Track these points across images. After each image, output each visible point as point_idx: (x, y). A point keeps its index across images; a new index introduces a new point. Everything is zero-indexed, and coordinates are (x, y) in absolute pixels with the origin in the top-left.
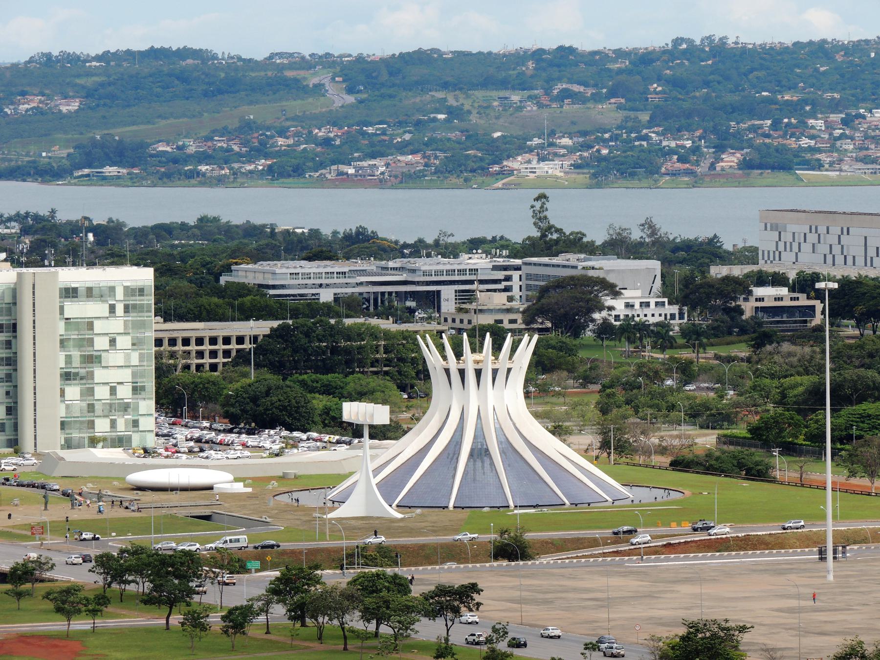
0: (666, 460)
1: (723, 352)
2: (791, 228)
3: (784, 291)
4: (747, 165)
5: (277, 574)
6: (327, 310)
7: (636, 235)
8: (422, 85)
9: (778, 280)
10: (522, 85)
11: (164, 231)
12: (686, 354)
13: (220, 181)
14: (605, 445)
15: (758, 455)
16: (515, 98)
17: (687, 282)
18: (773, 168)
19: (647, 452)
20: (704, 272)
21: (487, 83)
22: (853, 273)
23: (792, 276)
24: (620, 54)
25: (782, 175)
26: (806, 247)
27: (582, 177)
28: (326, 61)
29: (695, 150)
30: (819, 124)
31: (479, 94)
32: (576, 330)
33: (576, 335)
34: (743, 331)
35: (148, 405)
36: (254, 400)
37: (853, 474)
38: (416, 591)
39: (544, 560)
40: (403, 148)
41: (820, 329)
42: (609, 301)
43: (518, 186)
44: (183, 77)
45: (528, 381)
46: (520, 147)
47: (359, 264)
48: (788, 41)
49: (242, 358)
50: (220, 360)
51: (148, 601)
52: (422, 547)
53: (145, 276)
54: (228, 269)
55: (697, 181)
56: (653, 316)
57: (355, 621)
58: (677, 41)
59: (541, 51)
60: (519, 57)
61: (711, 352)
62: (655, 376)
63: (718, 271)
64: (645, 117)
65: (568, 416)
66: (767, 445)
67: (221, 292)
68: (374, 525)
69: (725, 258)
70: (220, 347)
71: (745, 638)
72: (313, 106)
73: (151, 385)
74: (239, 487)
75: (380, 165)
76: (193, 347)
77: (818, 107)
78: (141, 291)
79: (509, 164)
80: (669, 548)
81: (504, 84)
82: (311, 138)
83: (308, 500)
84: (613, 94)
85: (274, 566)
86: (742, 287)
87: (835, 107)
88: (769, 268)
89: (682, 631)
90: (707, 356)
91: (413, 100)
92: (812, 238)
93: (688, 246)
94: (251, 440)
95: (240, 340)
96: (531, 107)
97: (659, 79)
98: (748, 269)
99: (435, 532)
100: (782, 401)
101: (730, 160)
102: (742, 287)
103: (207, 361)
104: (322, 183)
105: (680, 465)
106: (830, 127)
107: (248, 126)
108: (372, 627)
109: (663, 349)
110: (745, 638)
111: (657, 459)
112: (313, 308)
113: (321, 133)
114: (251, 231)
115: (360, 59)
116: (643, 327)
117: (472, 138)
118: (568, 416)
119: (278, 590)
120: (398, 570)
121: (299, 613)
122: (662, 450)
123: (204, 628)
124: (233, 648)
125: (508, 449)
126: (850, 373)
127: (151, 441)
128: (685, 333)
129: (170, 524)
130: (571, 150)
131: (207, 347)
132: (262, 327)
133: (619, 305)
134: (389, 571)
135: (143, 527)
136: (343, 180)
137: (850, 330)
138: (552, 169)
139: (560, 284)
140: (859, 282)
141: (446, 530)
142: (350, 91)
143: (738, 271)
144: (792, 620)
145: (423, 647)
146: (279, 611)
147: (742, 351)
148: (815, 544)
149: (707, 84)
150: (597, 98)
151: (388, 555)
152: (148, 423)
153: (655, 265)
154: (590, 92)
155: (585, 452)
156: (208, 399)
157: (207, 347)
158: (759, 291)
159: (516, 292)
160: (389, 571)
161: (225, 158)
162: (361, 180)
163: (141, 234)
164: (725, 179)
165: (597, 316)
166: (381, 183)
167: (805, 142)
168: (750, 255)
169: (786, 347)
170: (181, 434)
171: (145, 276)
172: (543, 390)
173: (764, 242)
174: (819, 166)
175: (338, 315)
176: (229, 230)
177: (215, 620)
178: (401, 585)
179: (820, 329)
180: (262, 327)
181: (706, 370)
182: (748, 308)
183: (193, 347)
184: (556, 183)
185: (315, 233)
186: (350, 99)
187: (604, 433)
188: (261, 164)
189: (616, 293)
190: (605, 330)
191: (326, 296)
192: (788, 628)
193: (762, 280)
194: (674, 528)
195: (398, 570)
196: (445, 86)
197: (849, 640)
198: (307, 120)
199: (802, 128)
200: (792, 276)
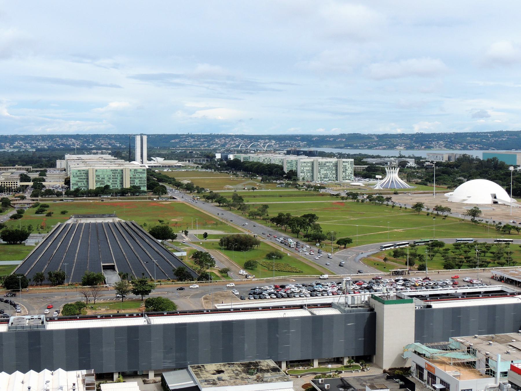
0: (415, 183)
1: (422, 170)
2: (430, 155)
3: (429, 163)
4: (425, 148)
5: (367, 196)
6: (374, 164)
7: (411, 156)
8: (386, 138)
9: (429, 162)
10: (398, 138)
11: (355, 155)
12: (417, 170)
13: (362, 149)
14: (407, 181)
15: (426, 182)
16: (397, 139)
17: (418, 162)
18: (428, 148)
19: (412, 182)
20: (420, 161)
21: (394, 138)
22: (438, 161)
23: (430, 161)
24: (410, 134)
25: (429, 149)
26: (432, 158)
27: (405, 149)
28: (374, 135)
29: (419, 146)
30: (434, 143)
31: (393, 139)
32: (404, 167)
33: (404, 168)
34: (424, 168)
35: (353, 175)
36: (365, 175)
37: (437, 185)
38: (384, 198)
39: (400, 195)
40: (384, 145)
41: (434, 167)
42: (408, 164)
43: (397, 150)
44: (357, 136)
45: (398, 173)
46: (397, 145)
47: (378, 159)
48: (430, 133)
49: (364, 170)
50: (361, 170)
51: (352, 198)
52: (385, 193)
53: (353, 160)
54: (362, 159)
55: (419, 150)
56: (413, 166)
57: (377, 202)
58: (417, 133)
59: (400, 134)
60: (398, 135)
61: (420, 170)
62: (413, 173)
63: (421, 160)
64: (413, 142)
65: (403, 177)
66: (427, 181)
67: (361, 162)
68: (380, 190)
69: (422, 159)
70: (361, 169)
71: (424, 204)
72: (373, 140)
73: (353, 173)
74: (363, 185)
75: (381, 147)
76: (358, 169)
77: (434, 141)
78: (352, 162)
79: (396, 147)
80: (415, 193)
81: (396, 138)
82: (372, 144)
83: (372, 187)
84: (409, 139)
85: (367, 195)
86: (424, 162)
87: (436, 141)
88: (428, 160)
89: (416, 203)
90: (420, 171)
91: (385, 139)
92: (433, 157)
93: (418, 157)
94: (365, 180)
95: (364, 168)
96: (399, 141)
97: (415, 137)
98: (425, 160)
99: (387, 191)
100: (429, 176)
101: (423, 147)
102: (424, 162)
103: (360, 170)
104: (374, 149)
105: (416, 183)
106: (435, 143)
107: (365, 143)
108: (379, 202)
109: (414, 170)
110: (424, 204)
111: (414, 183)
112: (372, 164)
113: (374, 143)
114: (365, 155)
115: (379, 135)
116: (412, 167)
117: (392, 144)
118: (403, 177)
119: (368, 198)
120: (383, 195)
121: (370, 200)
122: (414, 182)
123: (359, 202)
124: (362, 204)
125: (396, 181)
126: (437, 173)
127: (353, 180)
128: (417, 168)
129: (355, 189)
130: (404, 146)
131: (360, 169)
132: (366, 166)
133: (409, 164)
134: (381, 195)
135: (352, 190)
136: (376, 149)
137: (437, 168)
138: (402, 148)
139: (402, 162)
140: (439, 162)
141: (388, 191)
142: (377, 138)
143: (424, 160)
144: (430, 202)
145: (385, 205)
146: (368, 200)
147: (424, 170)
148: (432, 193)
149: (420, 138)
150: (407, 140)
151: (381, 194)
152: (353, 177)
153: (414, 159)
154: (406, 139)
155: (405, 182)
156: (360, 175)
157: (360, 169)
158: (426, 163)
159: (397, 163)
160: (381, 195)
161: (362, 146)
162: (378, 149)
163: (352, 155)
164: (423, 149)
165: (407, 166)
166: (381, 149)
167: (432, 145)
168: (425, 159)
169: (430, 170)
170: (356, 179)
171: (353, 160)
172: (400, 174)
173: (427, 157)
174: (434, 148)
175: (376, 165)
176: (363, 155)
177: (360, 201)
178: (382, 197)
179: (434, 167)
180: (366, 166)
181: (420, 173)
182: (425, 165)
183: (358, 169)
184: (402, 150)
185: (373, 155)
186: (377, 139)
187: (407, 179)
188: (367, 147)
189: (409, 163)
190: (408, 167)
191: (374, 163)
192: (429, 203)
193: (427, 161)
194: (416, 191)
195: (383, 195)
196: (389, 138)
197: (436, 205)
198: (372, 142)
199: (432, 144)
200: (430, 161)
